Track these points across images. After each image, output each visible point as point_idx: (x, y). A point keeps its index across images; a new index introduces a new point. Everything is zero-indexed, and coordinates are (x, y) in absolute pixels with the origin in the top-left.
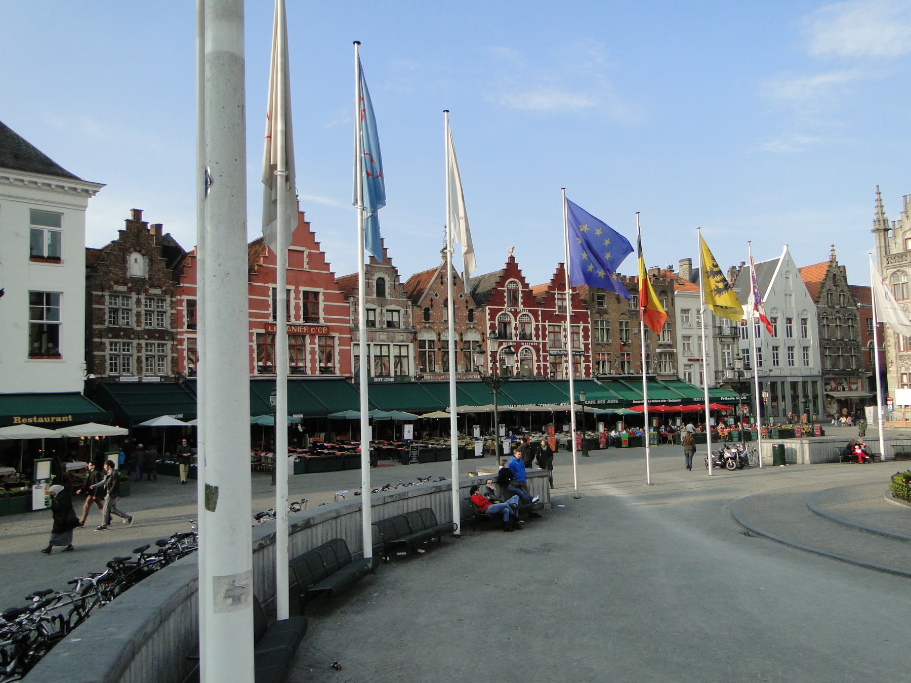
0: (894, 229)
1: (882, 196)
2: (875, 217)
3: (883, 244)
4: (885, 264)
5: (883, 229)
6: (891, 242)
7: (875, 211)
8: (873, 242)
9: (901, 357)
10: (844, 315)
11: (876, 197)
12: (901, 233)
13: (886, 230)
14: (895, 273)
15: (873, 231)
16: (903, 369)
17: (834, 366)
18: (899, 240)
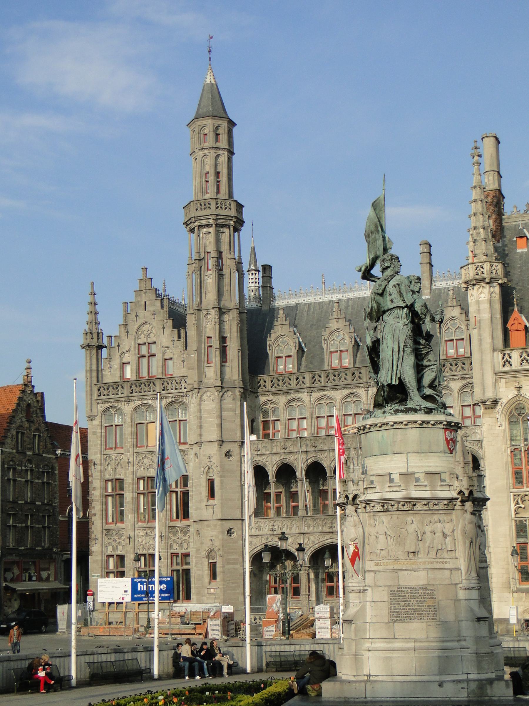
0: (110, 347)
1: (98, 299)
2: (87, 327)
3: (94, 367)
4: (95, 396)
5: (96, 345)
6: (105, 364)
7: (87, 318)
8: (80, 362)
9: (108, 531)
10: (37, 466)
11: (90, 299)
12: (118, 354)
13: (100, 347)
14: (107, 409)
15: (83, 347)
16: (110, 548)
17: (19, 541)
18: (115, 364)
